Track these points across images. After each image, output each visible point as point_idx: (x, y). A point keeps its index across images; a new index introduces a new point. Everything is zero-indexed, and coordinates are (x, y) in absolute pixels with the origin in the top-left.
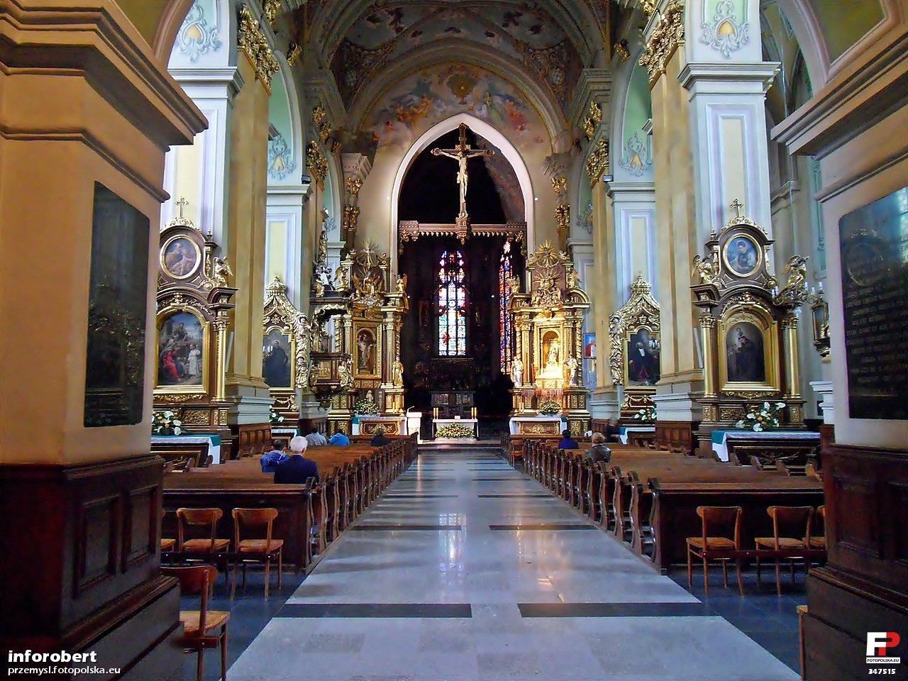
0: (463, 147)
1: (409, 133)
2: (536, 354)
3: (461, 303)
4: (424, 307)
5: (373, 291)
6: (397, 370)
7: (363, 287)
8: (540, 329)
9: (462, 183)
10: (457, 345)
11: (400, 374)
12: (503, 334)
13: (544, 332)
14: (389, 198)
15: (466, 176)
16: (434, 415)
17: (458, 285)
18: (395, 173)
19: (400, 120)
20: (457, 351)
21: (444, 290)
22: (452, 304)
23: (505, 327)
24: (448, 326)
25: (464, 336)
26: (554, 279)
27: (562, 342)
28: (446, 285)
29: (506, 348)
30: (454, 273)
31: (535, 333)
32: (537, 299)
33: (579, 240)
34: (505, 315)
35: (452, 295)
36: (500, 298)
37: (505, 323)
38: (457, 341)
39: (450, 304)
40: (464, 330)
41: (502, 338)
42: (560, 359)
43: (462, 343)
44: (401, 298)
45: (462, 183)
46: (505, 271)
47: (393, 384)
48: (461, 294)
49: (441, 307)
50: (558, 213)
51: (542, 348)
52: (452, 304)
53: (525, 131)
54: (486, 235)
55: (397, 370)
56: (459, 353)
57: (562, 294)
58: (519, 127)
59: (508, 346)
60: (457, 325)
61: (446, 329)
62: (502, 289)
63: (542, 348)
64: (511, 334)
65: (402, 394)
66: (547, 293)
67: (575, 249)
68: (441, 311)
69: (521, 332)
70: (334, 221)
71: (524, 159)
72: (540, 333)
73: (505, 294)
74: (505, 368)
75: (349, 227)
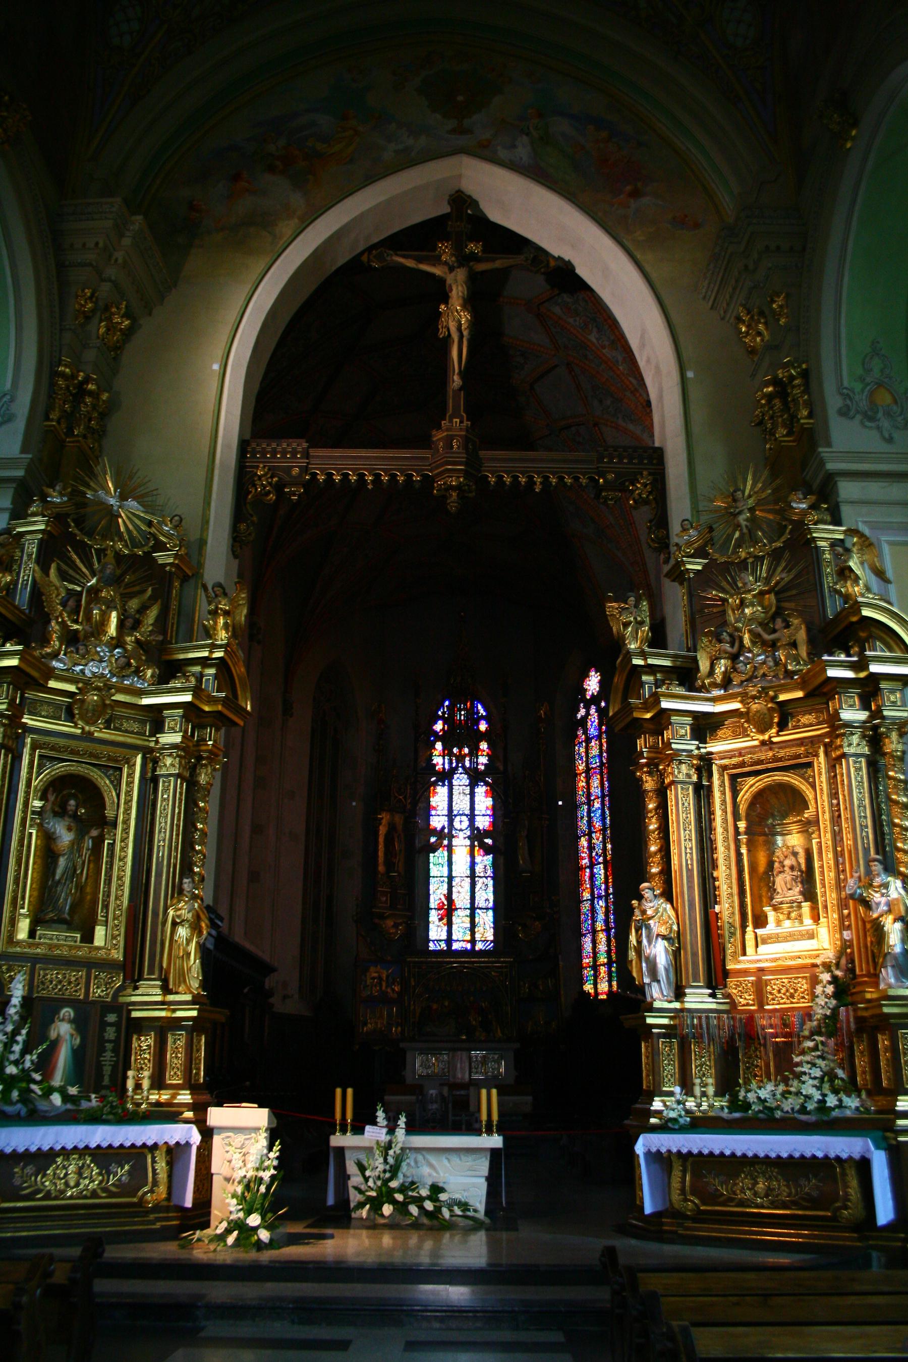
0: (458, 249)
1: (297, 200)
2: (724, 875)
3: (483, 823)
4: (392, 827)
5: (112, 630)
6: (183, 932)
7: (77, 611)
8: (734, 778)
9: (455, 336)
10: (473, 925)
11: (192, 948)
12: (586, 895)
13: (750, 787)
14: (216, 367)
15: (465, 318)
16: (338, 1116)
17: (475, 778)
18: (241, 302)
19: (271, 169)
20: (473, 941)
21: (442, 791)
22: (461, 823)
23: (592, 876)
24: (450, 878)
25: (491, 905)
26: (780, 592)
27: (825, 818)
28: (446, 777)
29: (594, 932)
30: (466, 750)
31: (717, 794)
32: (722, 667)
33: (860, 456)
34: (591, 848)
35: (462, 803)
36: (576, 807)
37: (592, 866)
38: (472, 917)
39: (456, 824)
40: (491, 889)
41: (585, 907)
42: (827, 894)
43: (486, 921)
44: (221, 664)
45: (455, 336)
46: (588, 740)
47: (166, 990)
48: (484, 802)
49: (434, 832)
50: (770, 397)
51: (744, 850)
52: (461, 823)
53: (646, 200)
54: (531, 482)
55: (183, 932)
56: (479, 946)
57: (812, 641)
58: (629, 188)
59: (600, 925)
60: (473, 876)
61: (446, 886)
62: (582, 784)
63: (744, 850)
64: (607, 894)
65: (196, 1026)
66: (755, 636)
67: (847, 490)
68: (433, 840)
69: (662, 793)
70: (12, 400)
71: (648, 268)
72: (735, 793)
73: (589, 794)
74: (595, 984)
75: (70, 432)
